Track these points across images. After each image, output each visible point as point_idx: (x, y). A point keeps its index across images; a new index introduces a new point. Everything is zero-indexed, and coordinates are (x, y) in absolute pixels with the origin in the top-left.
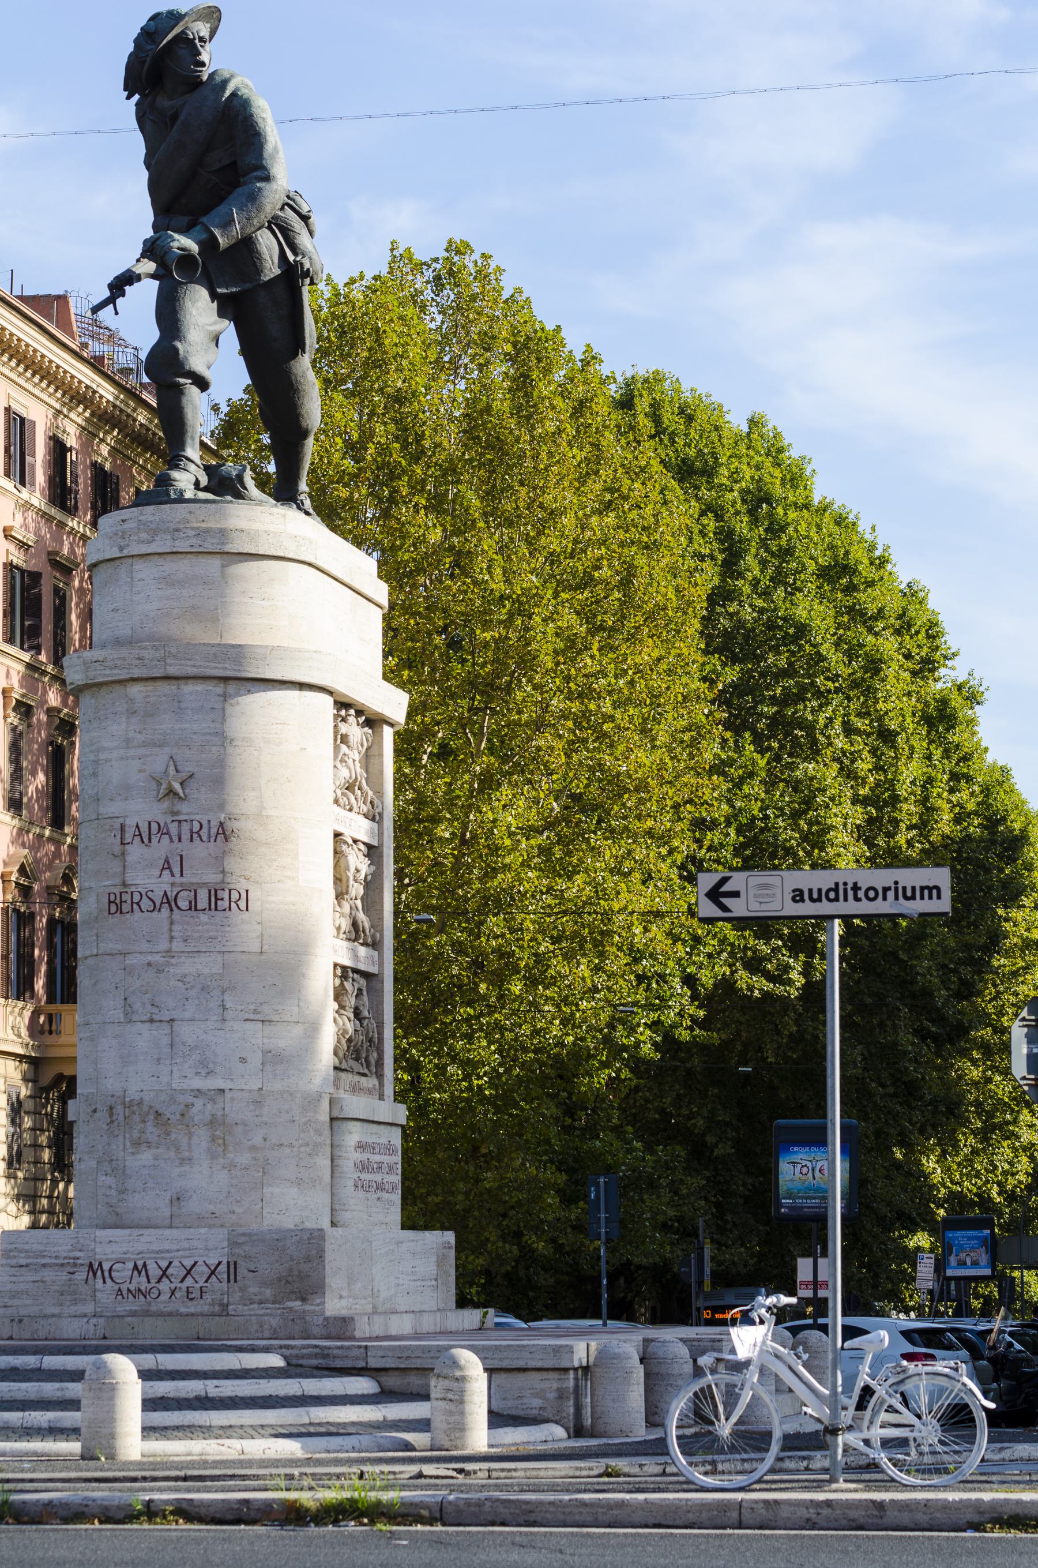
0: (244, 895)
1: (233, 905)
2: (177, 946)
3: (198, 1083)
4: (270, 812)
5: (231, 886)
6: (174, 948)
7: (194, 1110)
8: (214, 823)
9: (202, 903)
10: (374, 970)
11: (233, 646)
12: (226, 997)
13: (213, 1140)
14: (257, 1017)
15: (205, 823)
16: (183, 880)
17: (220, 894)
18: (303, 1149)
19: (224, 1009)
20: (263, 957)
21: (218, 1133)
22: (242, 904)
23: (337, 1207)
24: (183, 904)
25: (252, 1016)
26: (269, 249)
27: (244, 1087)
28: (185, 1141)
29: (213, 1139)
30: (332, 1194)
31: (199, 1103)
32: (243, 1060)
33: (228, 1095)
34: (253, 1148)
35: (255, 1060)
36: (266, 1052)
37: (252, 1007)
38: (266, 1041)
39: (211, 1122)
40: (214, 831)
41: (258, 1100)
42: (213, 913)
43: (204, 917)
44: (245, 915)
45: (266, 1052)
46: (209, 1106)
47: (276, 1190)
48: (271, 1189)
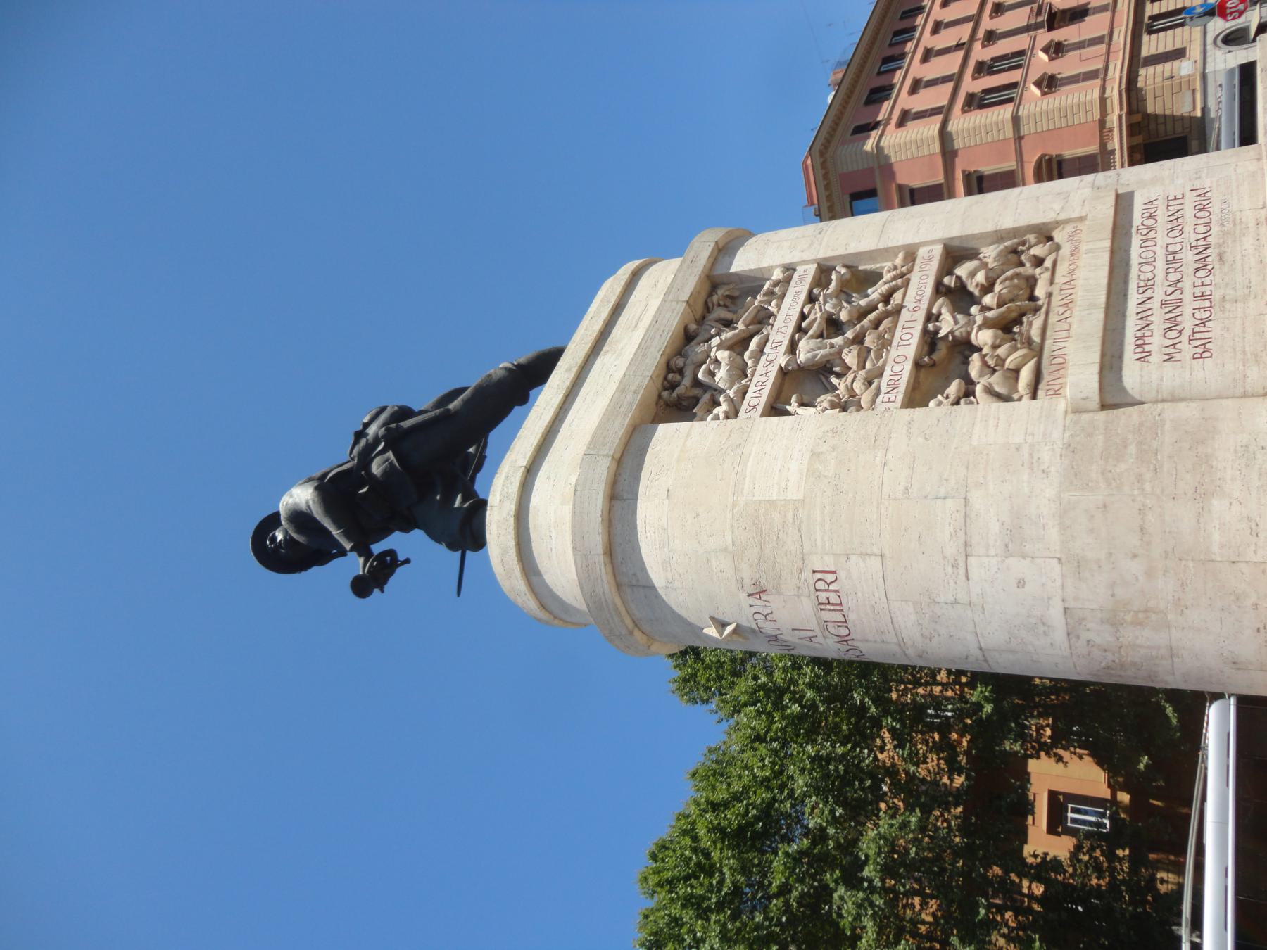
0: (819, 576)
1: (831, 587)
2: (891, 638)
3: (1059, 635)
4: (729, 541)
5: (812, 589)
6: (895, 640)
7: (1098, 640)
8: (751, 601)
9: (838, 617)
10: (938, 250)
11: (582, 588)
12: (942, 599)
13: (1140, 624)
14: (962, 564)
15: (754, 610)
16: (817, 629)
17: (824, 600)
18: (1148, 487)
19: (956, 602)
20: (887, 552)
21: (1128, 618)
22: (830, 577)
23: (1239, 391)
24: (844, 632)
25: (962, 571)
26: (379, 466)
27: (1058, 583)
28: (1143, 651)
29: (1138, 624)
30: (1220, 397)
31: (1085, 636)
32: (1021, 583)
33: (1071, 604)
34: (1150, 573)
35: (1018, 567)
36: (1007, 552)
37: (950, 569)
38: (992, 552)
39: (1113, 625)
40: (758, 602)
41: (1076, 565)
42: (844, 607)
43: (852, 617)
44: (842, 575)
45: (1007, 552)
46: (1090, 626)
47: (1216, 537)
48: (1215, 549)
